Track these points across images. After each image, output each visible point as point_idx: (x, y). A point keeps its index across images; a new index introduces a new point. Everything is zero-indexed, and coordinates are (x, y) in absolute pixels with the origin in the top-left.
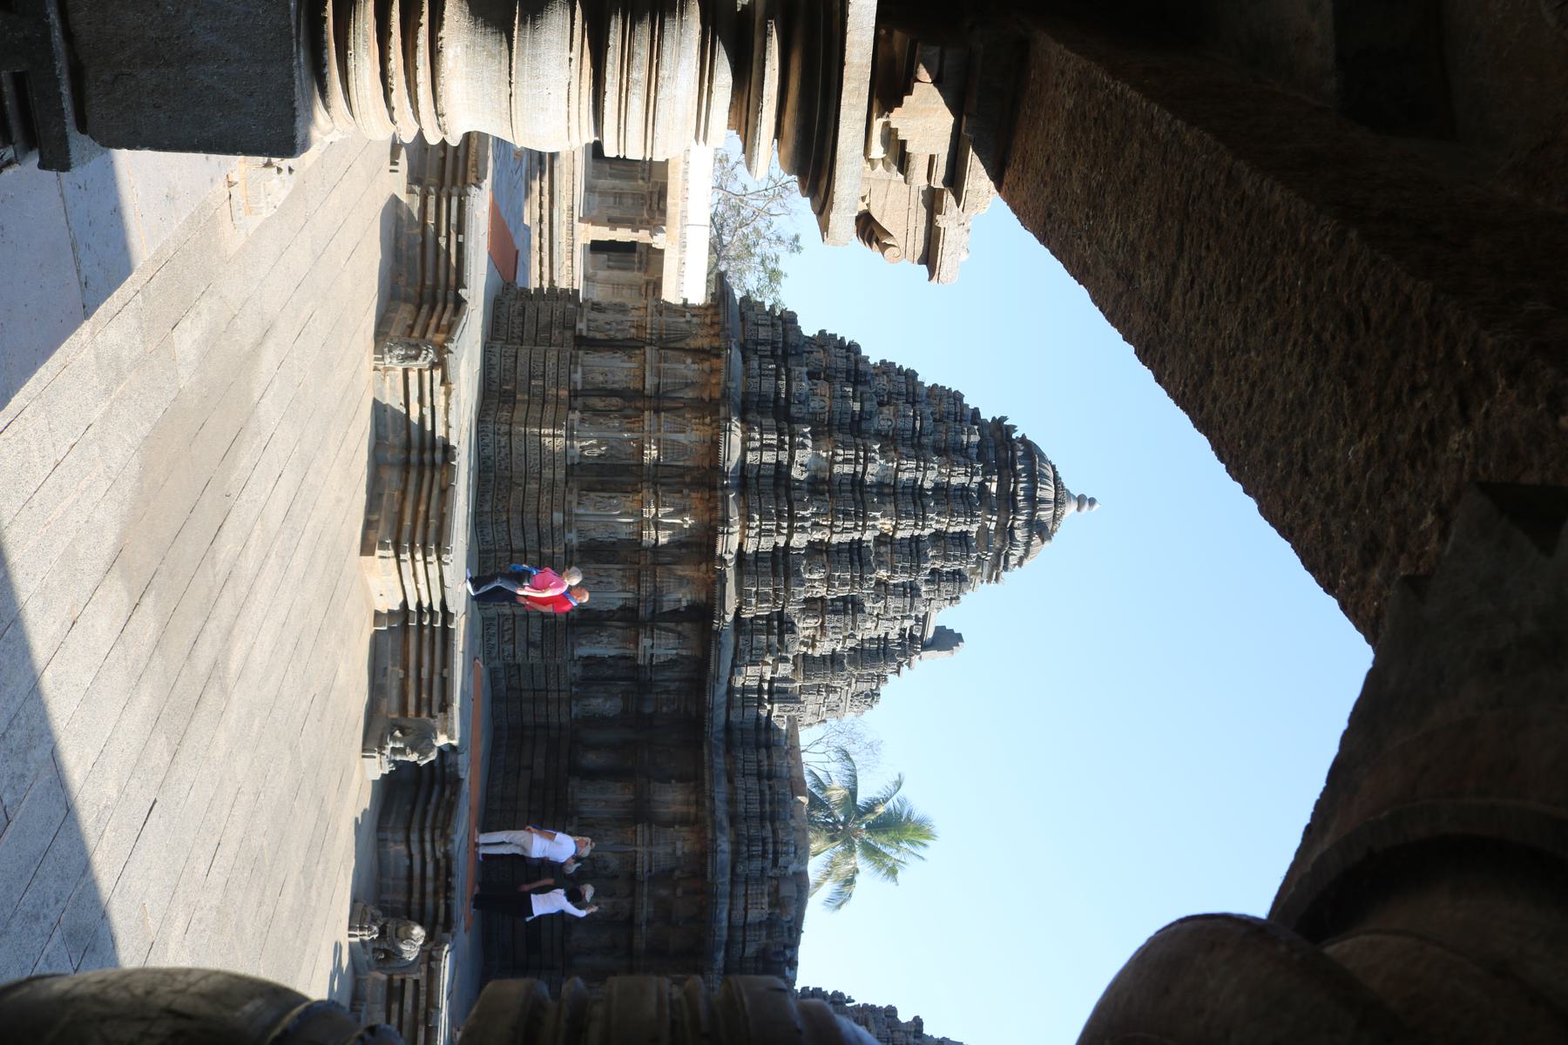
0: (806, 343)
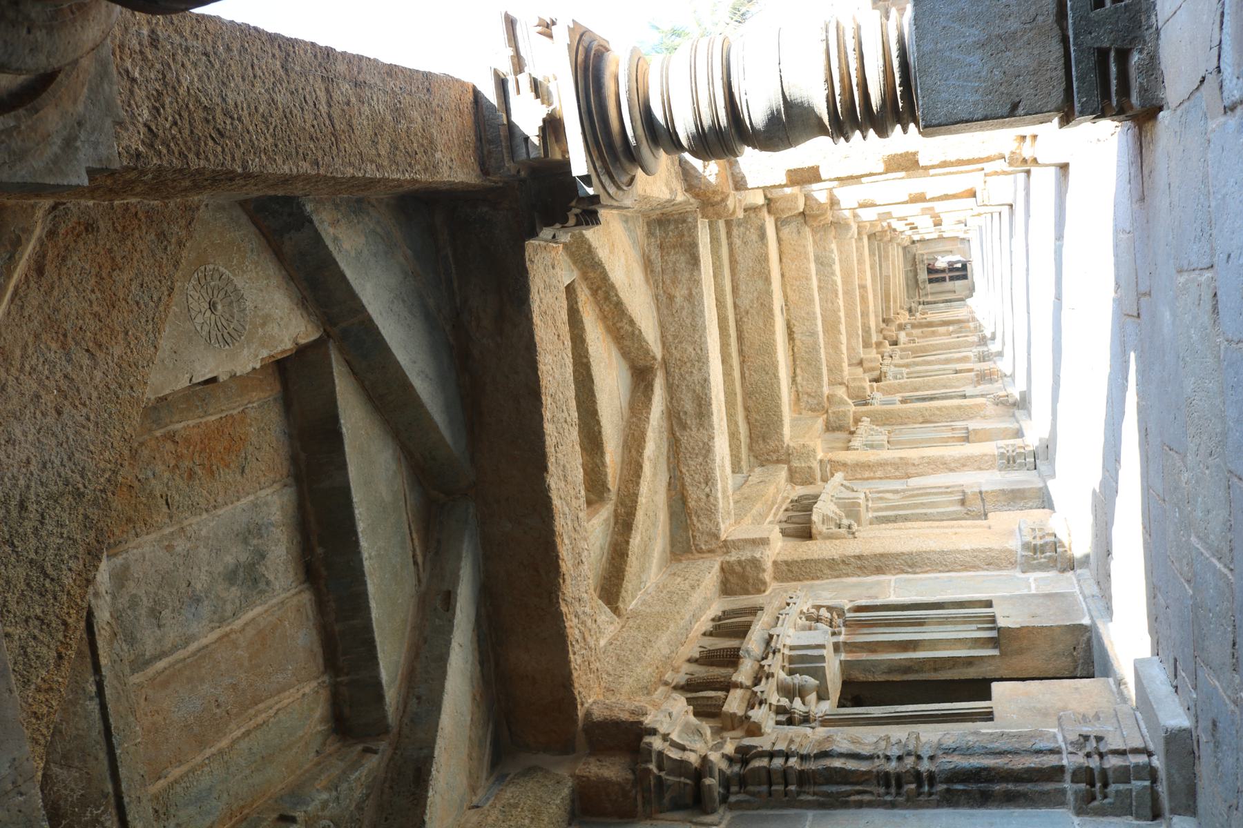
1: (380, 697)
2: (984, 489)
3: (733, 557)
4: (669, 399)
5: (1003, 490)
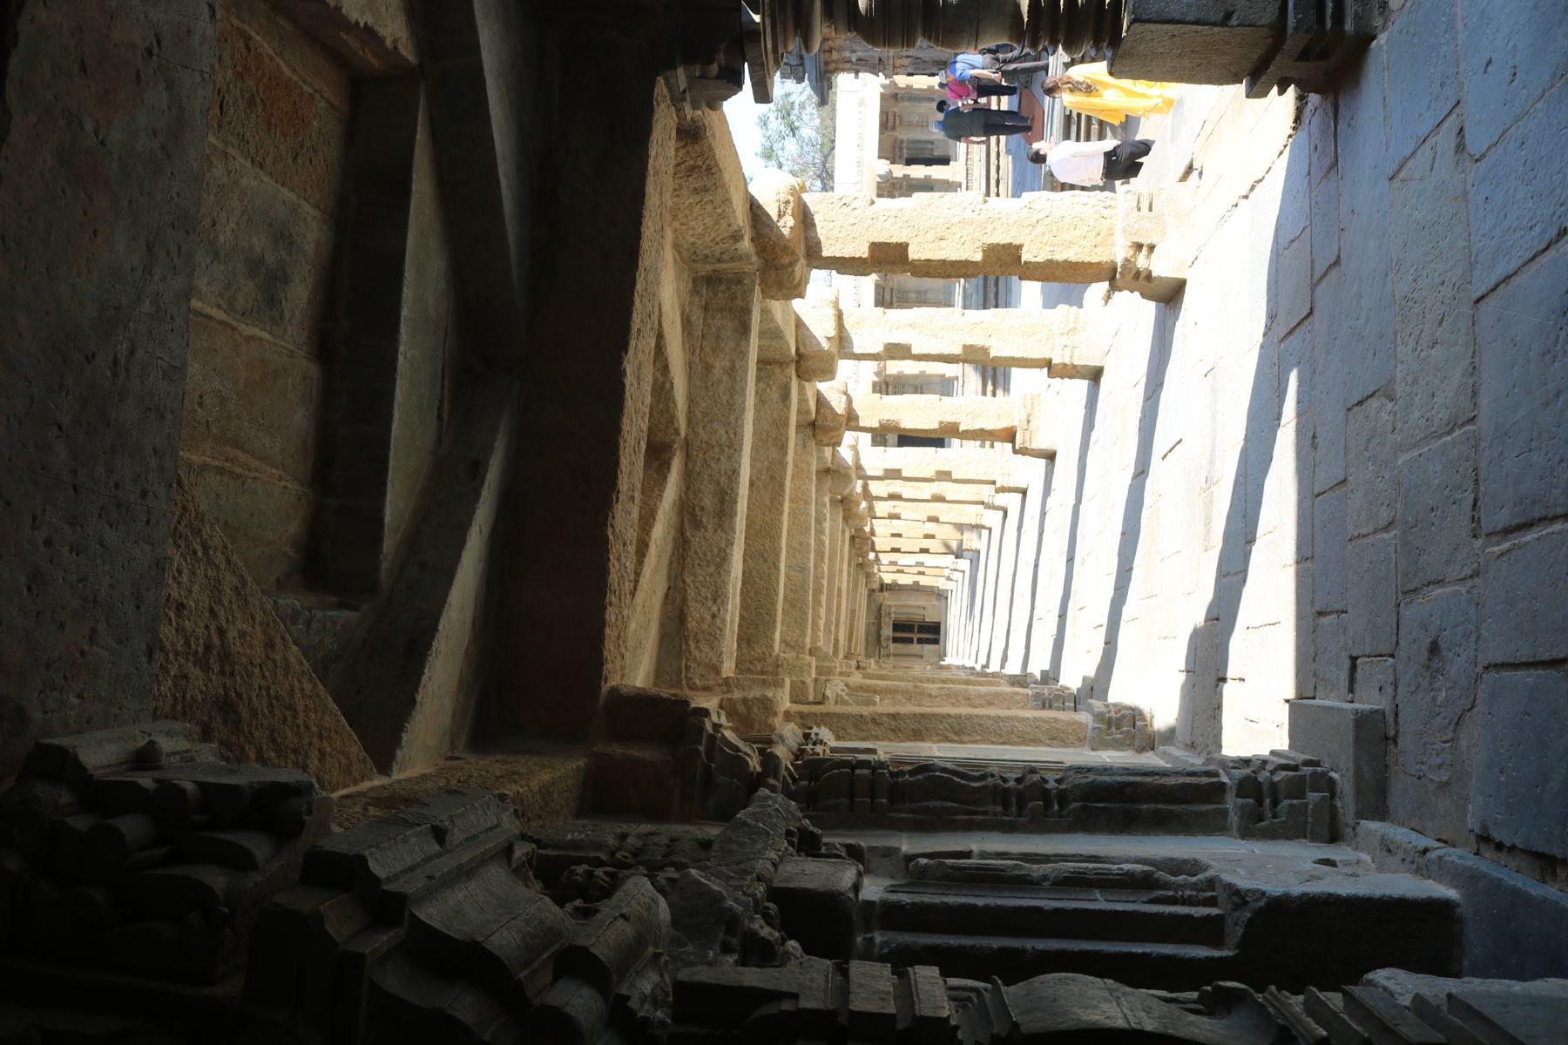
1: (378, 540)
4: (684, 489)
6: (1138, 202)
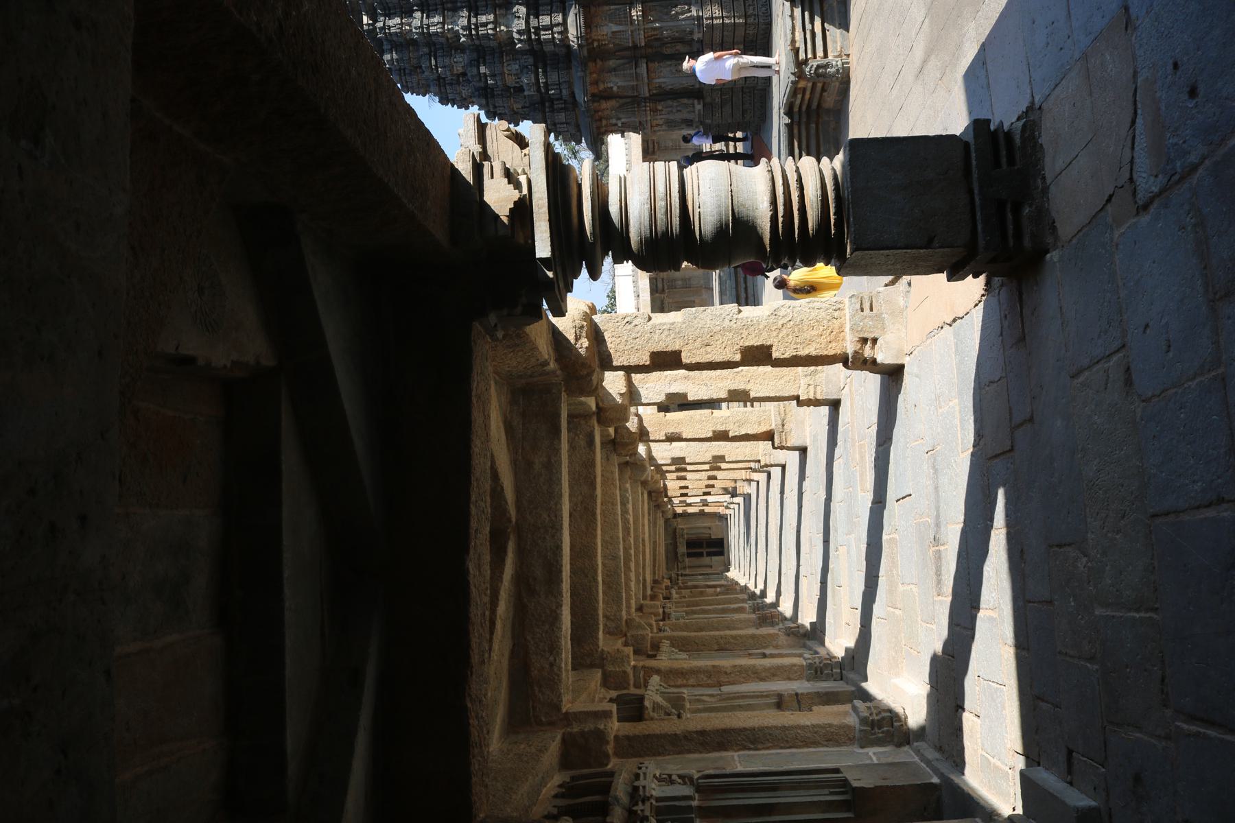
0: (528, 115)
2: (800, 691)
3: (576, 729)
5: (818, 692)
6: (861, 304)
